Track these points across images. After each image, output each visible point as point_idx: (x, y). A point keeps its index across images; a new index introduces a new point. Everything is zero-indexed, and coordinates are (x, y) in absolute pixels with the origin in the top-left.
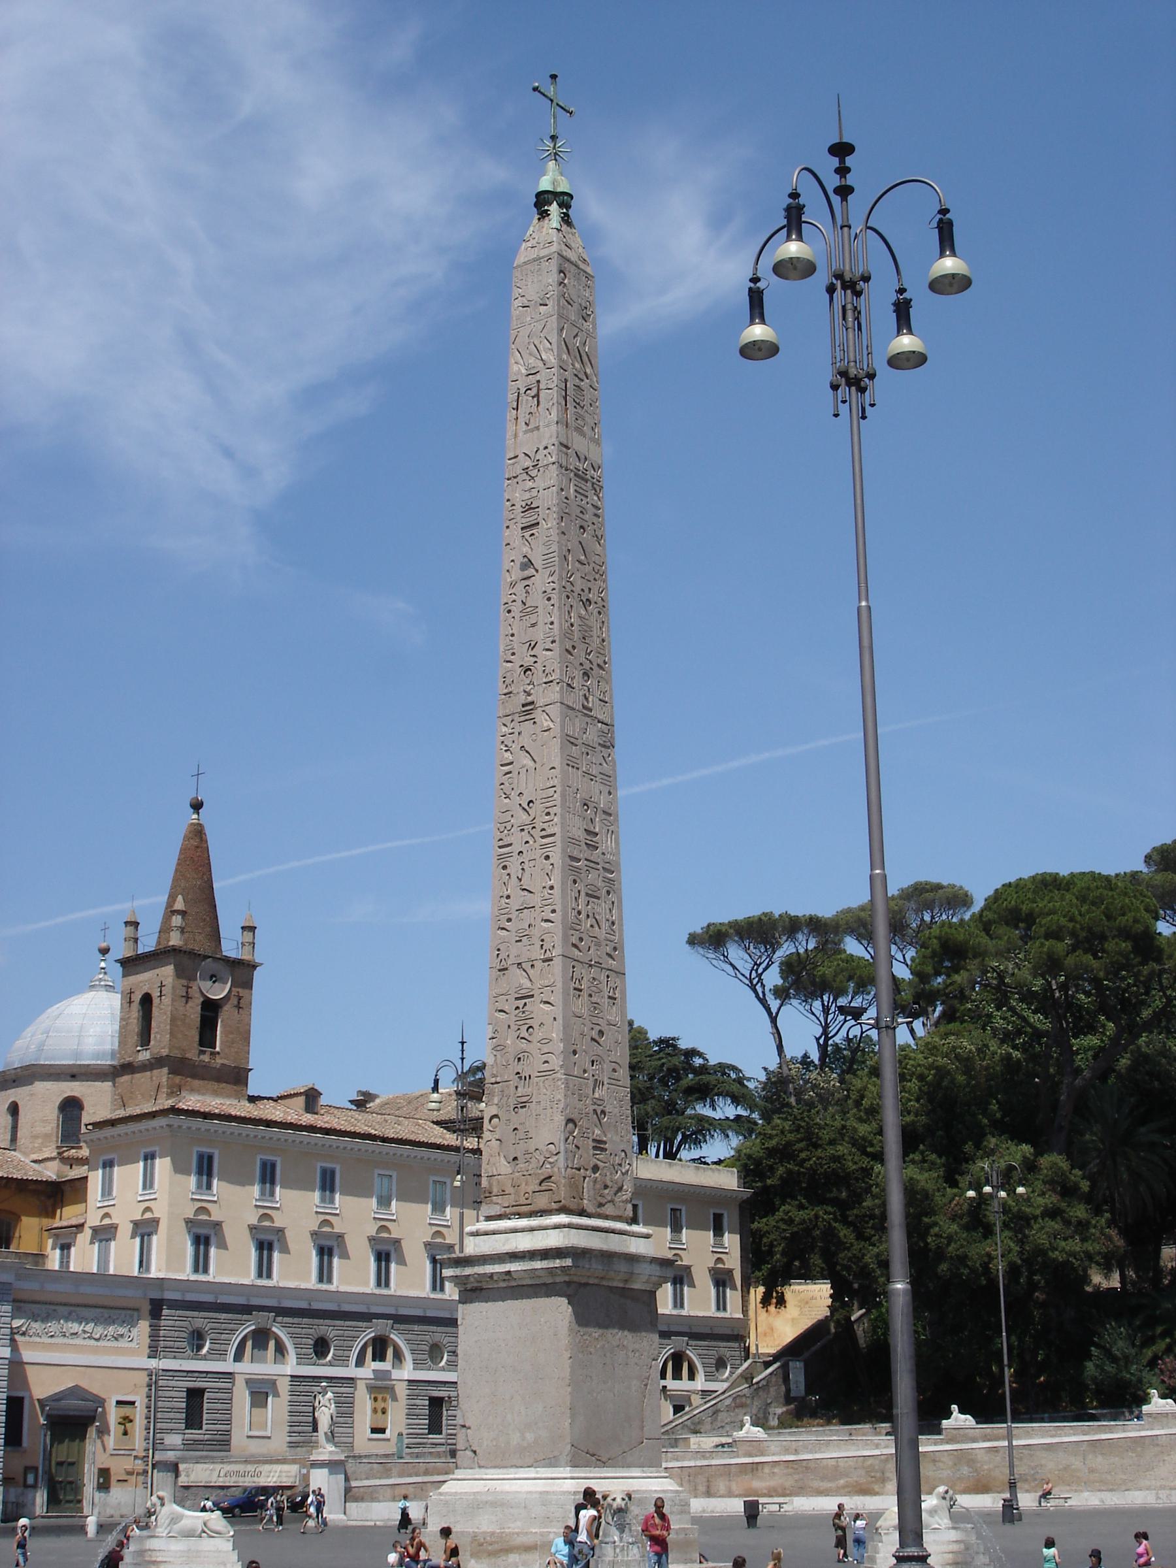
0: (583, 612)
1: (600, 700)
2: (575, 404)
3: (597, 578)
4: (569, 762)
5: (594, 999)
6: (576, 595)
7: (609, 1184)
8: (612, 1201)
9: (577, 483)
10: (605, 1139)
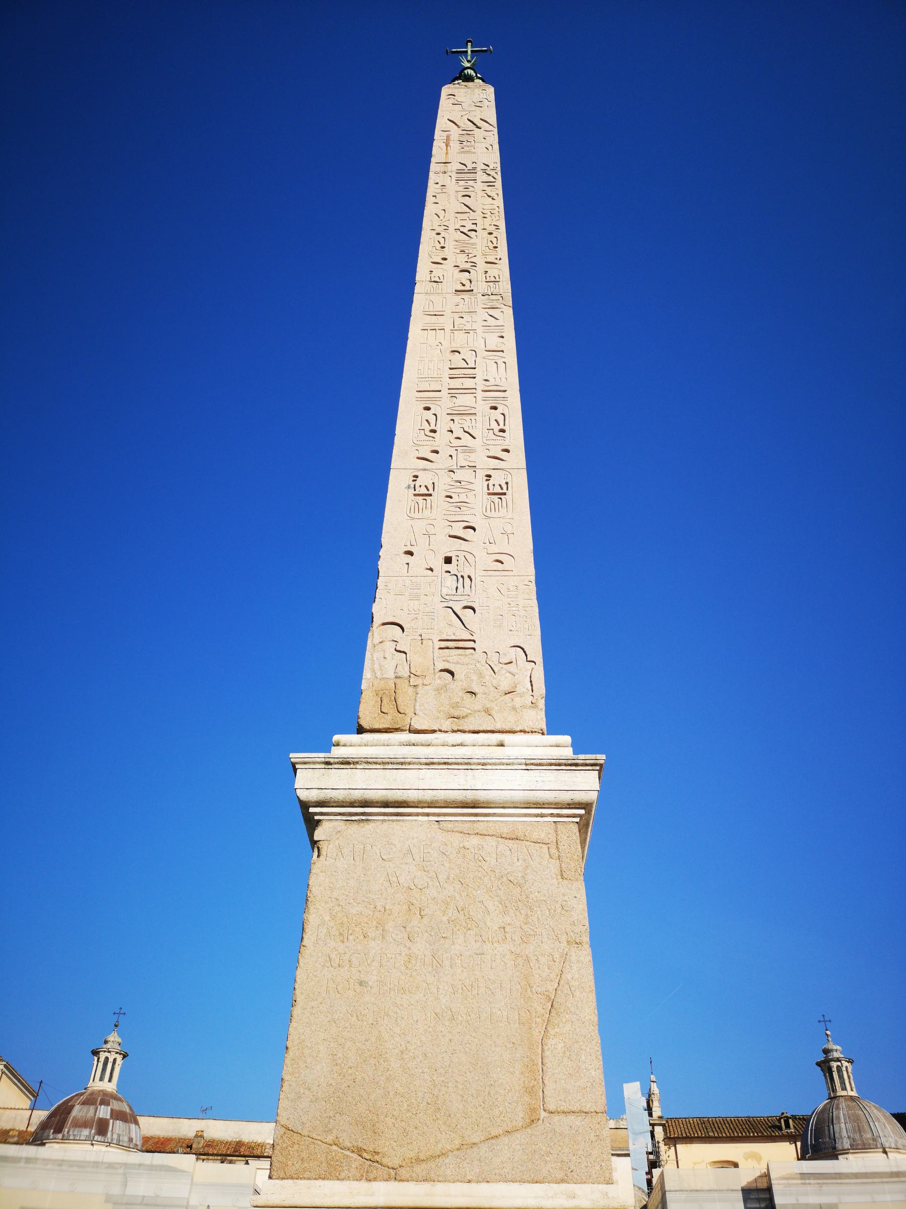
8: (487, 711)
10: (472, 638)
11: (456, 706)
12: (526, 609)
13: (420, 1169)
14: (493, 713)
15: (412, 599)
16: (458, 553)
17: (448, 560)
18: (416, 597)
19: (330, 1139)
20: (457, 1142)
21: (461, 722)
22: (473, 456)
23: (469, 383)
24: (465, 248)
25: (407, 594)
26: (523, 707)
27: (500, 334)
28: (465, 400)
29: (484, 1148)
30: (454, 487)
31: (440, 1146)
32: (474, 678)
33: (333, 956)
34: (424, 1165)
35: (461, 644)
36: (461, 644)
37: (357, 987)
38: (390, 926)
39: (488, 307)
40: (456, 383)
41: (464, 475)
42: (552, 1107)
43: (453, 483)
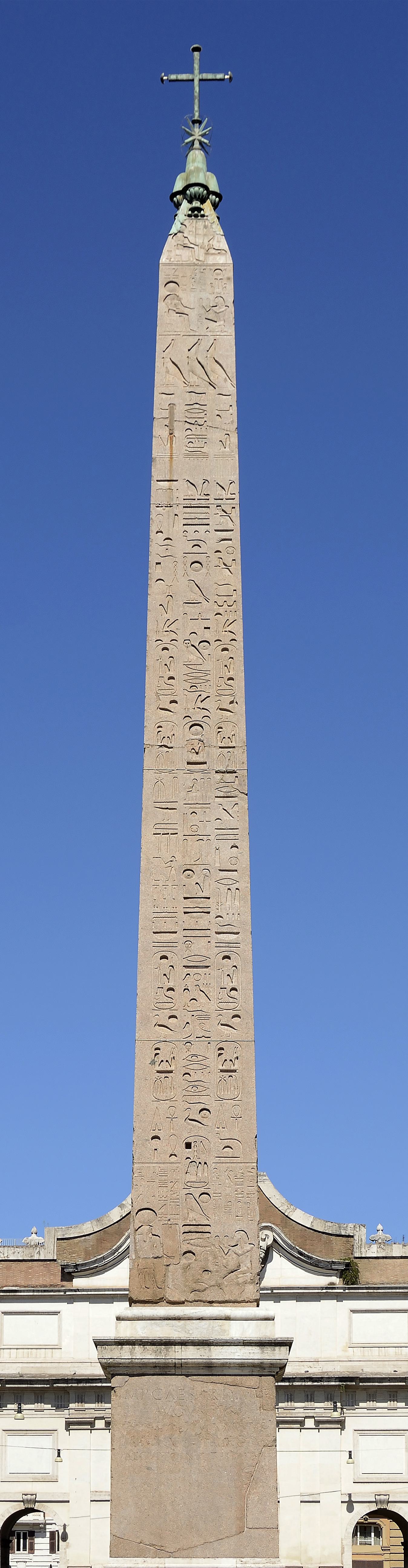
0: (193, 656)
1: (220, 747)
2: (188, 426)
3: (221, 610)
4: (158, 831)
5: (194, 1077)
6: (181, 641)
7: (211, 1267)
8: (219, 1286)
9: (187, 516)
10: (206, 1222)
11: (197, 1281)
12: (249, 1196)
13: (184, 1553)
14: (223, 1287)
15: (162, 1185)
16: (196, 1138)
17: (188, 1146)
18: (163, 1184)
19: (139, 1541)
20: (202, 1542)
21: (201, 1294)
22: (207, 1025)
23: (203, 921)
24: (197, 681)
25: (157, 1181)
26: (245, 1283)
27: (232, 843)
28: (199, 946)
29: (216, 1544)
30: (192, 1063)
31: (194, 1543)
32: (210, 1258)
33: (131, 1454)
34: (186, 1551)
35: (200, 1229)
36: (200, 1229)
37: (146, 1470)
38: (162, 1438)
39: (222, 794)
40: (189, 921)
41: (198, 1048)
42: (251, 1527)
43: (189, 1058)
